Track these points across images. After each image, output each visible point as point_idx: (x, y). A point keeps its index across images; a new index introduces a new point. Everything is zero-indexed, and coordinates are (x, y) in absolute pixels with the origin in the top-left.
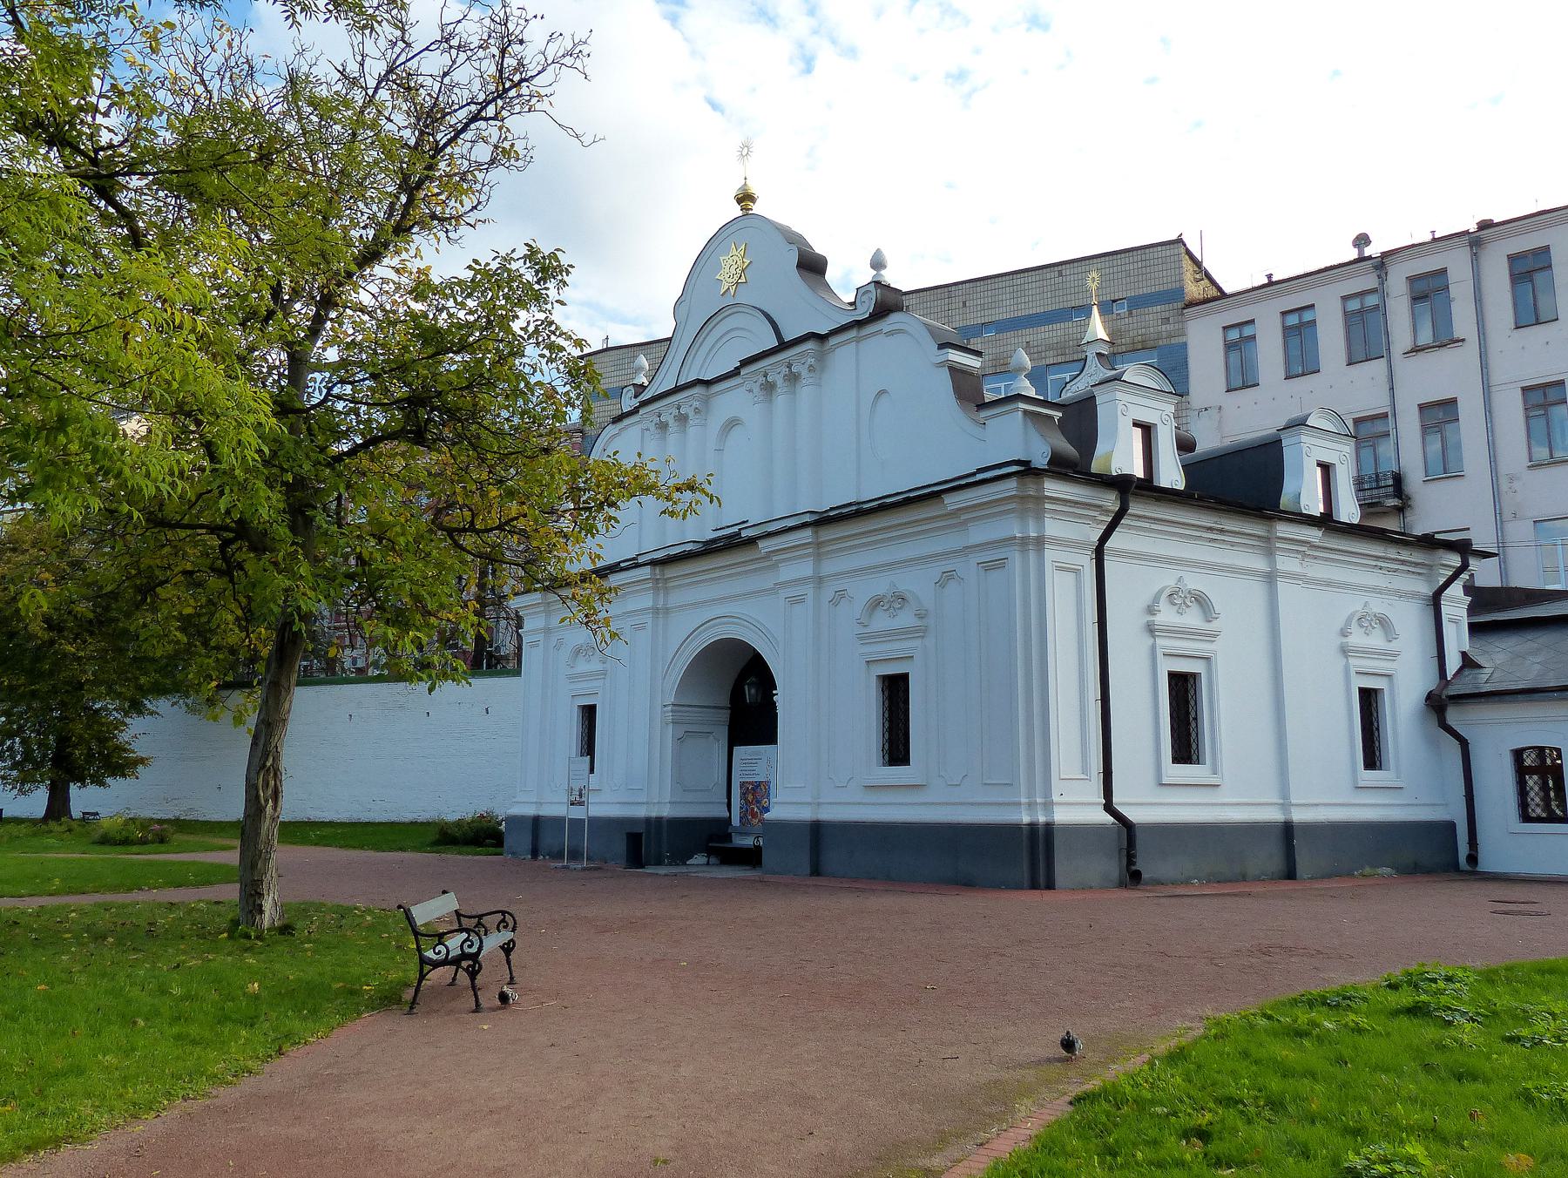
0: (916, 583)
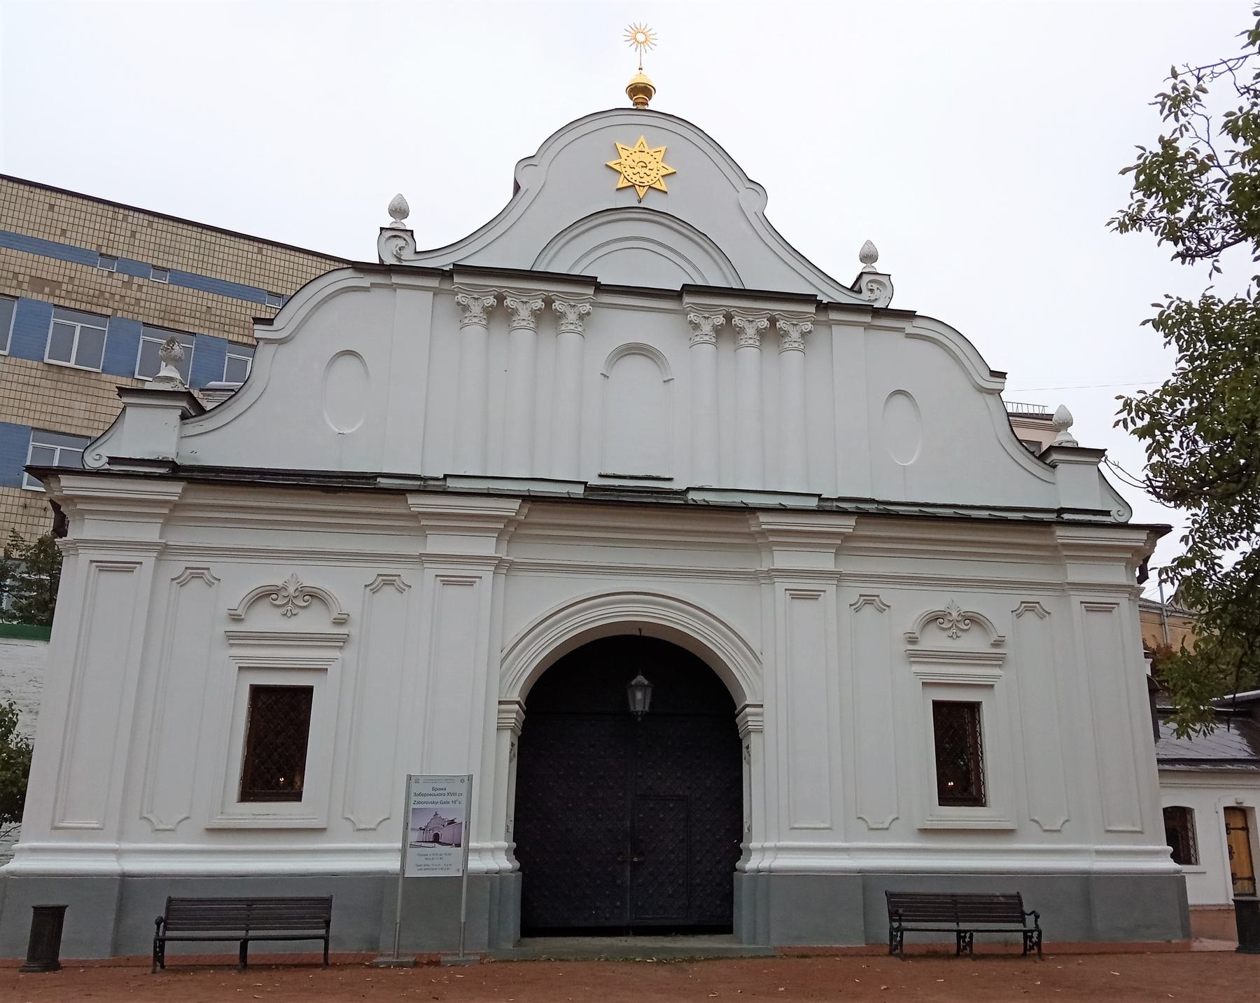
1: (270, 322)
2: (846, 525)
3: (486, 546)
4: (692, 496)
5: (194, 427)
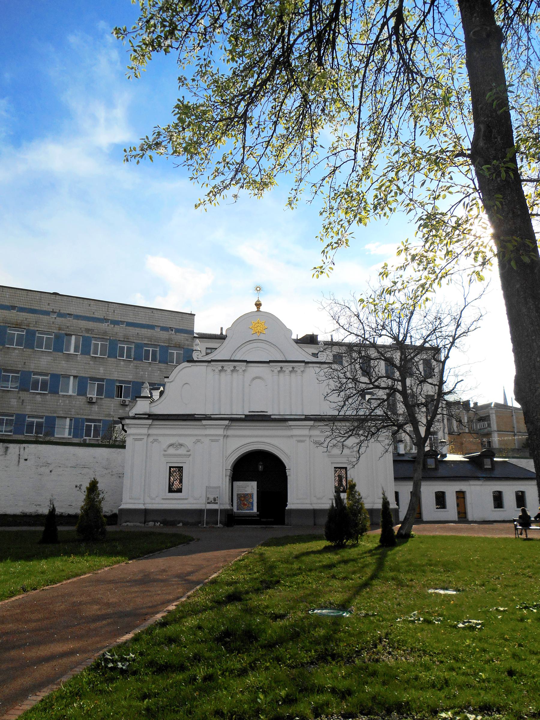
0: (188, 442)
1: (168, 377)
2: (311, 423)
3: (221, 432)
4: (272, 417)
5: (153, 405)
